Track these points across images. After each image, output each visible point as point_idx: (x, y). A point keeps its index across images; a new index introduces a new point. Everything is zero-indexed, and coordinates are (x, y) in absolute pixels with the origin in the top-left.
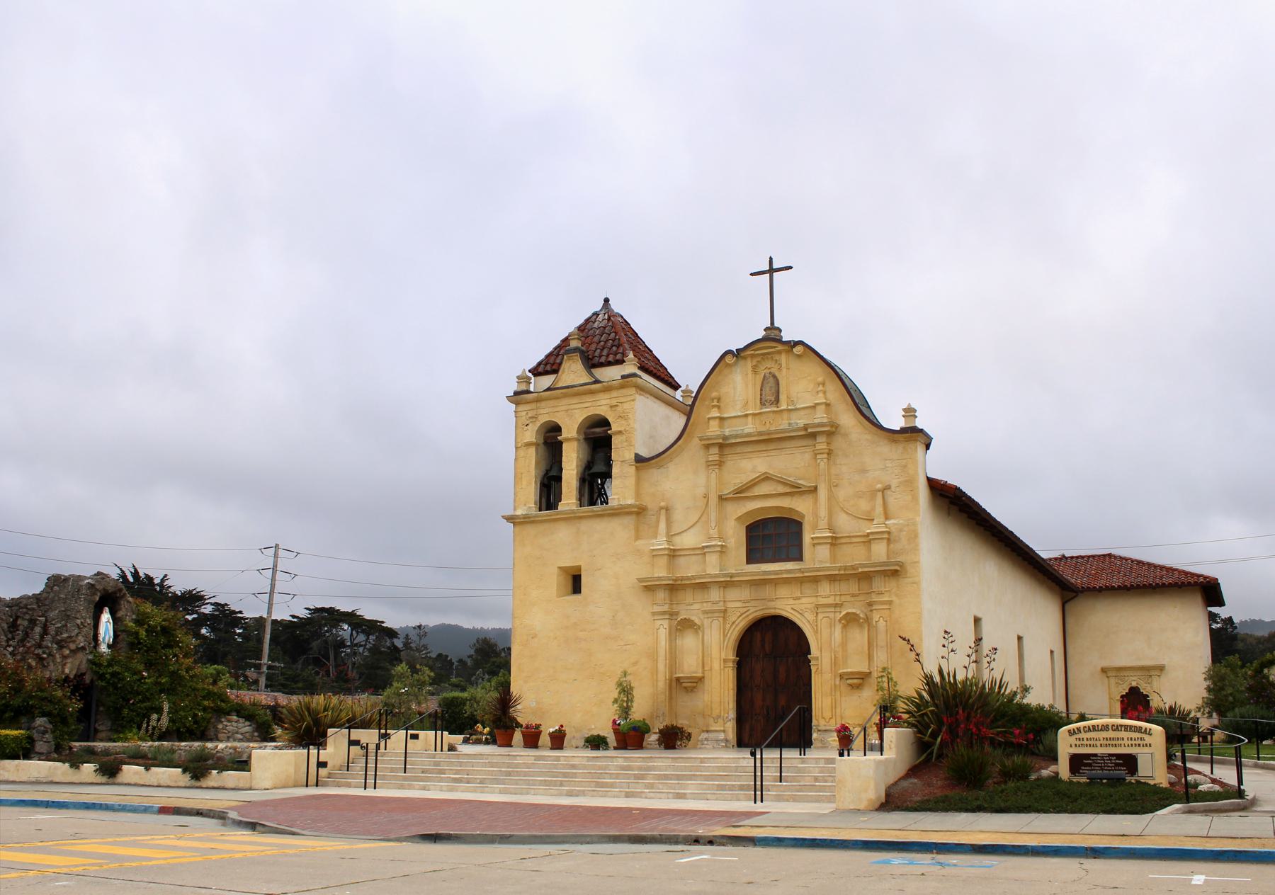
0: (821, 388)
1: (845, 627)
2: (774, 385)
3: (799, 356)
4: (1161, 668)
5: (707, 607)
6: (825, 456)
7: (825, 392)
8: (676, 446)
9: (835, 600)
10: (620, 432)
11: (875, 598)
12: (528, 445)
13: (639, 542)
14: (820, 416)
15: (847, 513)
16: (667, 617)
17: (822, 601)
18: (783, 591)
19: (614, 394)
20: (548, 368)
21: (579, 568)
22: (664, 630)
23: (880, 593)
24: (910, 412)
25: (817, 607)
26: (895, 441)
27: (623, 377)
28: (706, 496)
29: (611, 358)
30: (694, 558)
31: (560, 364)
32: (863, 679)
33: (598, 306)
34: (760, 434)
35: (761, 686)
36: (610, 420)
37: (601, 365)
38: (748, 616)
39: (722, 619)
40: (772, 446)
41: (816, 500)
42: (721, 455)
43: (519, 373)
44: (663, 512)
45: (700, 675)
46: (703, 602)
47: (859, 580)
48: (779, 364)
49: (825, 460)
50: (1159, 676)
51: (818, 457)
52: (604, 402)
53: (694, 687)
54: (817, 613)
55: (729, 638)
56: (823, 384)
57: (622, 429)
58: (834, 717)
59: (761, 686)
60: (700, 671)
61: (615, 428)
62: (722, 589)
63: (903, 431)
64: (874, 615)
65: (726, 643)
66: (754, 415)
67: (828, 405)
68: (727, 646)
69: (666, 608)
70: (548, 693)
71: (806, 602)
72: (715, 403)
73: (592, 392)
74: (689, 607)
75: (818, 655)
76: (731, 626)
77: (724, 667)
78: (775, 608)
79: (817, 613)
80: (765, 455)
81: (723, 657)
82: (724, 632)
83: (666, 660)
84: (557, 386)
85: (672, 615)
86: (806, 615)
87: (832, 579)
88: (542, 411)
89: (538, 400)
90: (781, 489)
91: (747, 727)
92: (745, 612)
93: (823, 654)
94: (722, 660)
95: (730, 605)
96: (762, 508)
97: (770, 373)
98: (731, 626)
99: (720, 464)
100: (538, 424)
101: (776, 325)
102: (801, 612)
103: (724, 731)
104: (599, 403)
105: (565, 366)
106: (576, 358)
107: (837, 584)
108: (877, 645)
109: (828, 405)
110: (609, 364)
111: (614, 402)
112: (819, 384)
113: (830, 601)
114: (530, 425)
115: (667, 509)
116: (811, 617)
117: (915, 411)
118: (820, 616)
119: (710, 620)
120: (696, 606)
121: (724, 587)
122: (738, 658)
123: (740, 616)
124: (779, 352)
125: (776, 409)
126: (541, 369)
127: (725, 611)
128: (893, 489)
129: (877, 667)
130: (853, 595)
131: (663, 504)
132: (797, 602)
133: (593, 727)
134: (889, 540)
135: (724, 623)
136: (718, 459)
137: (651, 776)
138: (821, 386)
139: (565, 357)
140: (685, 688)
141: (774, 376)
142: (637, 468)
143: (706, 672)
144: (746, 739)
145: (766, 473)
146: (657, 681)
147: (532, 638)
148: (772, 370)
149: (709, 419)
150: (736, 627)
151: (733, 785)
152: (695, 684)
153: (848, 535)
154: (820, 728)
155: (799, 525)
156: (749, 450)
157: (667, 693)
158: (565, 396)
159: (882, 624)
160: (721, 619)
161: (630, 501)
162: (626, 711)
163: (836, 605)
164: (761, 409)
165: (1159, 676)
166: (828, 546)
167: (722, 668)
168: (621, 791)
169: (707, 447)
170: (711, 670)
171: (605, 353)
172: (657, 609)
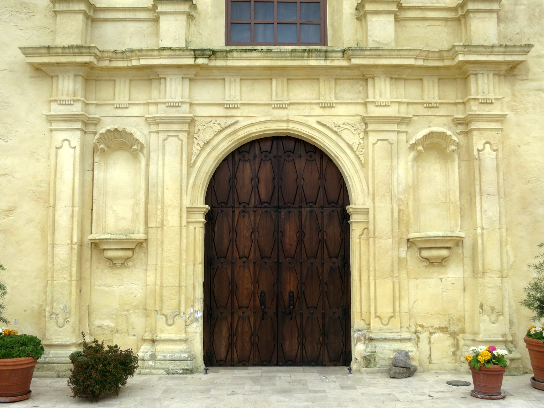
5: (153, 111)
9: (399, 112)
11: (475, 109)
16: (79, 125)
17: (374, 111)
22: (72, 150)
23: (487, 103)
25: (365, 121)
35: (252, 256)
38: (235, 132)
39: (186, 134)
45: (141, 236)
46: (148, 104)
53: (128, 259)
54: (366, 132)
55: (199, 170)
58: (397, 314)
59: (252, 256)
60: (142, 229)
62: (187, 82)
64: (475, 139)
68: (194, 184)
69: (77, 109)
74: (119, 112)
75: (368, 204)
76: (203, 149)
78: (288, 121)
79: (366, 132)
81: (187, 203)
82: (189, 160)
83: (73, 206)
86: (345, 134)
91: (224, 331)
92: (230, 126)
93: (377, 204)
94: (184, 211)
95: (200, 111)
98: (203, 149)
102: (335, 129)
103: (185, 341)
107: (401, 84)
113: (391, 111)
116: (354, 139)
118: (372, 138)
119: (162, 136)
120: (135, 111)
121: (190, 80)
122: (207, 206)
123: (220, 131)
127: (192, 122)
129: (483, 229)
130: (430, 106)
132: (327, 111)
135: (190, 144)
140: (110, 259)
143: (151, 231)
144: (222, 351)
146: (53, 245)
150: (213, 149)
152: (129, 253)
154: (372, 335)
157: (74, 269)
159: (488, 154)
160: (184, 136)
163: (403, 121)
167: (184, 223)
170: (162, 226)
172: (57, 110)
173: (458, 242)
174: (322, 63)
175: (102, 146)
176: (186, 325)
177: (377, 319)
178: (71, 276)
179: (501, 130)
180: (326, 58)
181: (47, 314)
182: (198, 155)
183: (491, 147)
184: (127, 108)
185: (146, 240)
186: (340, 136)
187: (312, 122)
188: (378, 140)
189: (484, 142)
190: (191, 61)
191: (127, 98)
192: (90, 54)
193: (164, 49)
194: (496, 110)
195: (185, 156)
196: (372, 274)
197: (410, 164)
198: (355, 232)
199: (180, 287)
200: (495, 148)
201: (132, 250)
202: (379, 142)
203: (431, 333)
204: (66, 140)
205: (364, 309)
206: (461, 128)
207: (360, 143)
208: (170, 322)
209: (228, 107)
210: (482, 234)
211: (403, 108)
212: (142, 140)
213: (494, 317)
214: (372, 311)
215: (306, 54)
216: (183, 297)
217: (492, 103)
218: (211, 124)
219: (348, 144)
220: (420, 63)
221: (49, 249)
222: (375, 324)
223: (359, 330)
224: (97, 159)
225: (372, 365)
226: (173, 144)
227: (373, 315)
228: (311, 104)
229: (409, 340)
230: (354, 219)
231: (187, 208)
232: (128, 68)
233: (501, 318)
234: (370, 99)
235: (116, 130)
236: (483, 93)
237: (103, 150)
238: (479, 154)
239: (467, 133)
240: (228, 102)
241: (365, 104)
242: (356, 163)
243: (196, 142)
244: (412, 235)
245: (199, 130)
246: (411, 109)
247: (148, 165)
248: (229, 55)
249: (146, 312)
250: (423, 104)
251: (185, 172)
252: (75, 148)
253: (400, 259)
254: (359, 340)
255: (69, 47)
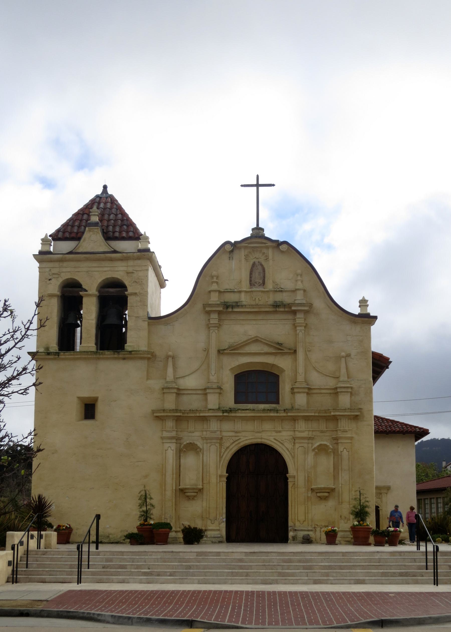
0: (299, 278)
1: (316, 454)
2: (262, 271)
3: (282, 252)
4: (388, 488)
6: (303, 328)
7: (302, 282)
8: (183, 309)
9: (308, 435)
10: (135, 294)
11: (340, 434)
12: (51, 296)
13: (149, 382)
14: (299, 297)
15: (318, 372)
16: (174, 441)
17: (298, 434)
18: (267, 426)
19: (131, 263)
20: (67, 235)
21: (96, 399)
22: (172, 451)
23: (345, 431)
24: (363, 303)
25: (294, 438)
26: (355, 323)
27: (140, 251)
28: (207, 350)
29: (124, 234)
30: (195, 397)
31: (83, 233)
32: (328, 492)
33: (99, 191)
34: (252, 306)
36: (127, 283)
37: (116, 239)
38: (239, 443)
39: (219, 444)
40: (260, 317)
41: (295, 360)
42: (220, 320)
43: (43, 237)
44: (170, 359)
45: (200, 487)
47: (326, 420)
48: (266, 256)
49: (303, 332)
50: (386, 493)
51: (298, 328)
52: (121, 269)
54: (294, 443)
55: (224, 459)
56: (301, 275)
57: (137, 291)
58: (307, 520)
61: (130, 290)
62: (219, 422)
63: (360, 316)
64: (339, 447)
65: (221, 464)
66: (246, 292)
67: (305, 291)
69: (174, 434)
70: (67, 498)
71: (286, 434)
72: (215, 280)
73: (111, 260)
74: (190, 434)
75: (295, 474)
76: (226, 450)
77: (220, 481)
78: (262, 438)
79: (294, 443)
80: (274, 323)
81: (219, 473)
82: (220, 455)
83: (173, 474)
84: (76, 251)
85: (178, 439)
86: (286, 444)
87: (307, 419)
88: (64, 270)
89: (61, 261)
90: (266, 349)
95: (224, 434)
96: (251, 362)
97: (259, 262)
98: (226, 450)
99: (219, 326)
100: (61, 280)
101: (260, 226)
102: (281, 442)
103: (219, 530)
104: (116, 269)
105: (86, 235)
106: (96, 230)
108: (341, 468)
109: (305, 291)
110: (123, 239)
111: (130, 269)
112: (297, 275)
113: (305, 434)
114: (53, 280)
115: (173, 358)
116: (289, 446)
117: (367, 301)
118: (297, 446)
119: (209, 445)
120: (197, 434)
121: (220, 420)
122: (227, 474)
123: (233, 443)
124: (267, 248)
125: (263, 290)
126: (60, 235)
127: (222, 438)
128: (352, 356)
129: (342, 484)
130: (322, 432)
131: (170, 353)
132: (279, 434)
133: (108, 526)
134: (351, 393)
136: (217, 322)
137: (317, 567)
138: (299, 276)
139: (87, 228)
140: (188, 496)
141: (262, 265)
142: (149, 324)
143: (204, 485)
145: (257, 337)
146: (165, 490)
147: (53, 453)
148: (260, 260)
149: (210, 292)
151: (394, 573)
153: (319, 387)
154: (296, 528)
155: (277, 377)
156: (242, 318)
157: (174, 501)
158: (87, 260)
159: (345, 453)
160: (218, 445)
161: (144, 348)
162: (146, 515)
163: (309, 438)
164: (251, 288)
165: (386, 493)
166: (305, 395)
167: (218, 481)
168: (310, 579)
169: (208, 313)
170: (209, 483)
171: (117, 229)
172: (165, 434)
173: (333, 490)
174: (276, 415)
175: (185, 450)
176: (219, 524)
177: (299, 522)
178: (172, 503)
179: (351, 443)
180: (277, 413)
181: (163, 519)
182: (224, 453)
183: (346, 450)
184: (193, 432)
185: (203, 489)
186: (284, 445)
187: (272, 439)
188: (300, 446)
189: (343, 448)
190: (221, 414)
191: (194, 429)
192: (180, 412)
193: (210, 409)
194: (349, 435)
195: (218, 453)
196: (296, 503)
197: (313, 457)
198: (290, 485)
199: (217, 508)
200: (348, 451)
201: (197, 492)
202: (300, 448)
203: (321, 528)
204: (170, 447)
205: (293, 518)
206: (335, 441)
207: (292, 448)
208: (213, 522)
209: (236, 432)
210: (342, 487)
211: (310, 433)
212: (201, 447)
213: (346, 521)
214: (296, 518)
215: (269, 411)
216: (218, 512)
217: (347, 432)
218: (229, 440)
219: (287, 448)
220: (317, 414)
221: (164, 492)
222: (297, 524)
223: (291, 527)
224: (182, 455)
225: (295, 540)
226: (213, 448)
227: (296, 520)
228: (271, 431)
229: (312, 530)
230: (289, 480)
231: (220, 475)
232: (195, 416)
233: (349, 521)
234: (296, 429)
235: (191, 443)
236: (343, 427)
237: (185, 451)
238: (341, 453)
239: (337, 444)
240: (236, 430)
241: (294, 431)
242: (290, 456)
243: (223, 447)
244: (313, 487)
245: (224, 442)
246: (314, 433)
247: (203, 457)
248: (237, 411)
249: (202, 518)
250: (319, 431)
251: (218, 460)
252: (173, 450)
253: (308, 497)
254: (291, 530)
255: (172, 410)
